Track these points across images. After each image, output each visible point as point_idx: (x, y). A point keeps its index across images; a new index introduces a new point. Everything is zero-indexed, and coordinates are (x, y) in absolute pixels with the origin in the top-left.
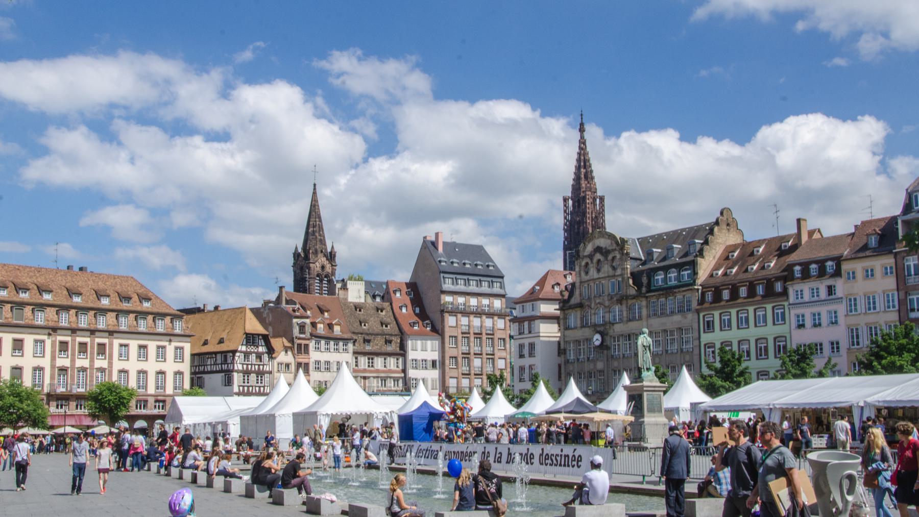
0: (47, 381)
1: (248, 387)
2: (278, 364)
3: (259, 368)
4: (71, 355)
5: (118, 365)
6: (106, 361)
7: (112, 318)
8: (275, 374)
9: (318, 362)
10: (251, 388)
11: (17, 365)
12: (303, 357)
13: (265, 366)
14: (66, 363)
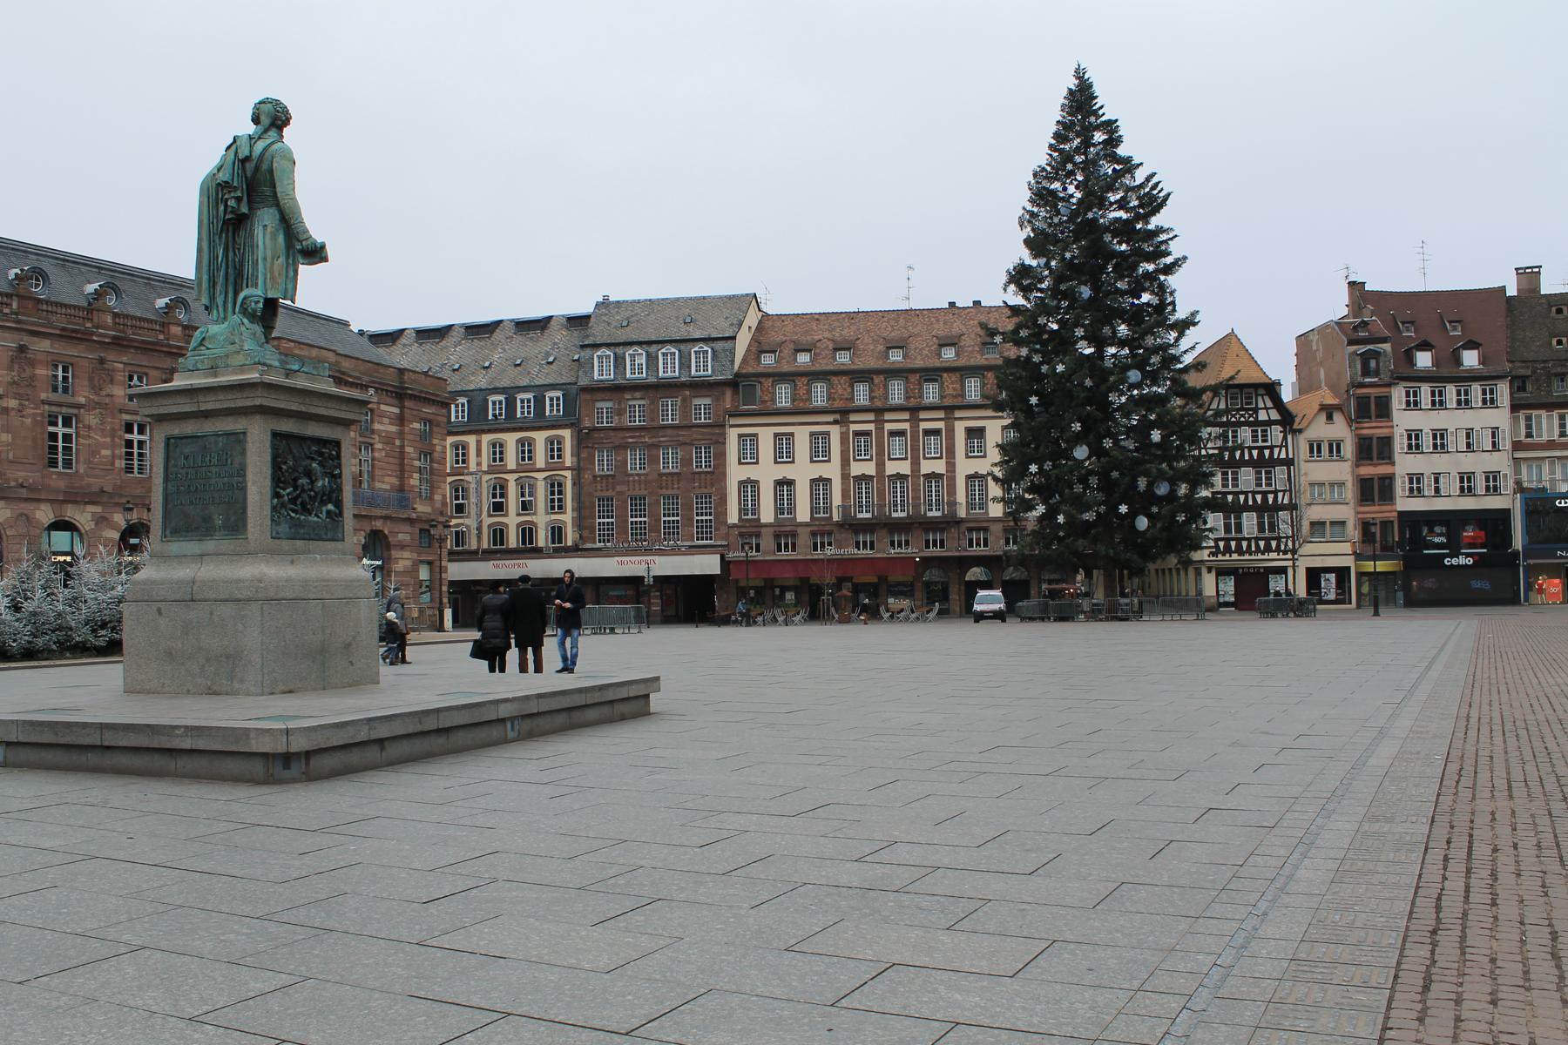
0: (837, 500)
1: (1236, 494)
2: (1311, 447)
3: (1261, 454)
4: (876, 455)
5: (965, 467)
6: (944, 460)
7: (952, 383)
8: (1304, 467)
9: (1414, 436)
10: (1242, 498)
11: (785, 477)
12: (1374, 425)
13: (1276, 451)
14: (869, 469)
